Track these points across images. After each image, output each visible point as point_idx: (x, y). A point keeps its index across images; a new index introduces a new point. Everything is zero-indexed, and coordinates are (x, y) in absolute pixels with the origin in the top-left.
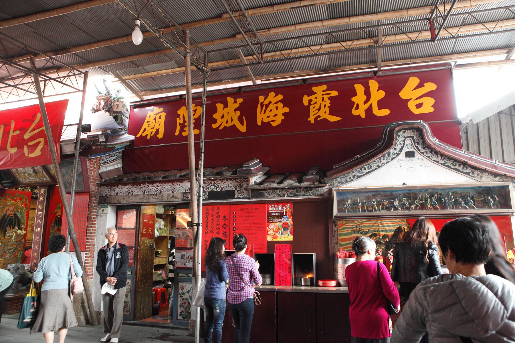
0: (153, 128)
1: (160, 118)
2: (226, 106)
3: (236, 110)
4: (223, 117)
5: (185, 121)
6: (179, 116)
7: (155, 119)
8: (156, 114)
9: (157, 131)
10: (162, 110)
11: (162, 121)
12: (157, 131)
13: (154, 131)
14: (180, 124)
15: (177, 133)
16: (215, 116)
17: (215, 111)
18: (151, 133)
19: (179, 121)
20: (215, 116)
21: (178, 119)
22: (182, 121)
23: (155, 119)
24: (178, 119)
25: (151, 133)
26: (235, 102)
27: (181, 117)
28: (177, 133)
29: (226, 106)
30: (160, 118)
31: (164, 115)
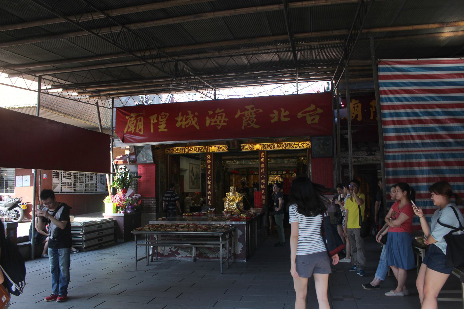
1: (357, 107)
6: (372, 107)
8: (354, 104)
9: (357, 116)
10: (358, 101)
11: (360, 109)
12: (357, 116)
13: (354, 116)
14: (373, 112)
18: (352, 117)
19: (372, 110)
21: (371, 109)
22: (374, 110)
23: (354, 107)
24: (371, 109)
25: (352, 117)
28: (372, 118)
30: (357, 107)
31: (360, 105)
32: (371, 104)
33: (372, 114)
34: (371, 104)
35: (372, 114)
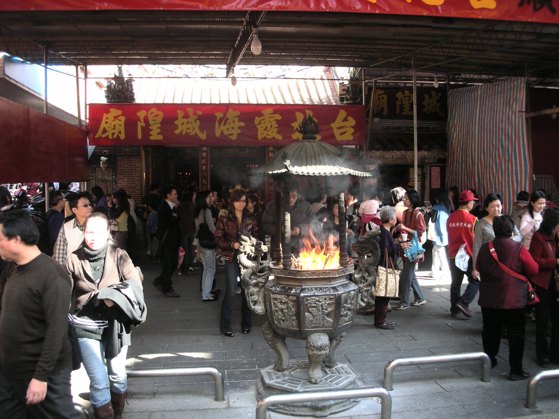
0: (379, 106)
2: (431, 97)
3: (438, 101)
4: (429, 104)
5: (403, 104)
6: (397, 99)
7: (379, 99)
8: (379, 95)
9: (382, 109)
11: (385, 101)
12: (382, 109)
13: (379, 108)
14: (399, 106)
15: (398, 112)
16: (424, 103)
17: (424, 99)
19: (398, 103)
20: (424, 103)
22: (400, 103)
23: (379, 99)
26: (437, 95)
27: (399, 100)
28: (398, 112)
29: (431, 97)
30: (383, 98)
31: (385, 96)
32: (397, 96)
33: (398, 108)
34: (397, 96)
35: (398, 108)
